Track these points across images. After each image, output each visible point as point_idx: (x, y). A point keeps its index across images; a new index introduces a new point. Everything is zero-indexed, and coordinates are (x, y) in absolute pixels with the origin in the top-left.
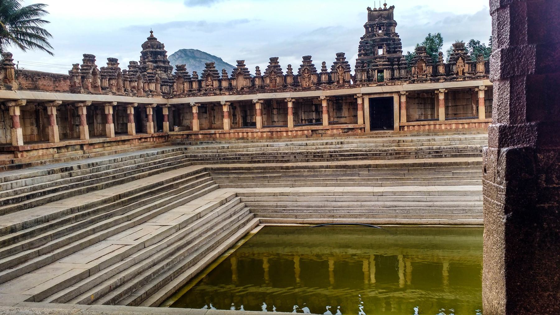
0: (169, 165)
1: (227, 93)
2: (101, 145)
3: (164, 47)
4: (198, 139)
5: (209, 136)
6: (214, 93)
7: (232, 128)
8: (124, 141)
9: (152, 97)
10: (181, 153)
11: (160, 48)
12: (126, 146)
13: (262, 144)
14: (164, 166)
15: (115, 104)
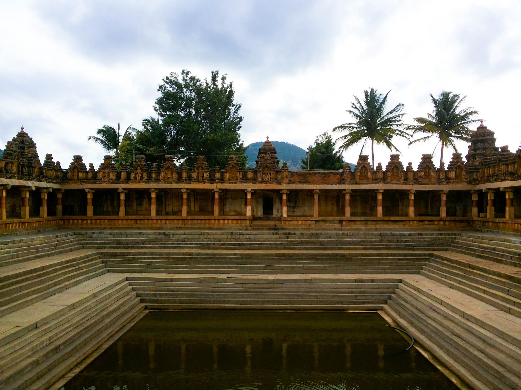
0: (407, 245)
1: (510, 179)
2: (363, 222)
3: (492, 134)
4: (488, 227)
5: (495, 224)
6: (501, 179)
7: (516, 217)
8: (396, 221)
9: (448, 183)
10: (450, 238)
11: (483, 136)
12: (397, 226)
13: (507, 238)
14: (397, 245)
15: (382, 191)
